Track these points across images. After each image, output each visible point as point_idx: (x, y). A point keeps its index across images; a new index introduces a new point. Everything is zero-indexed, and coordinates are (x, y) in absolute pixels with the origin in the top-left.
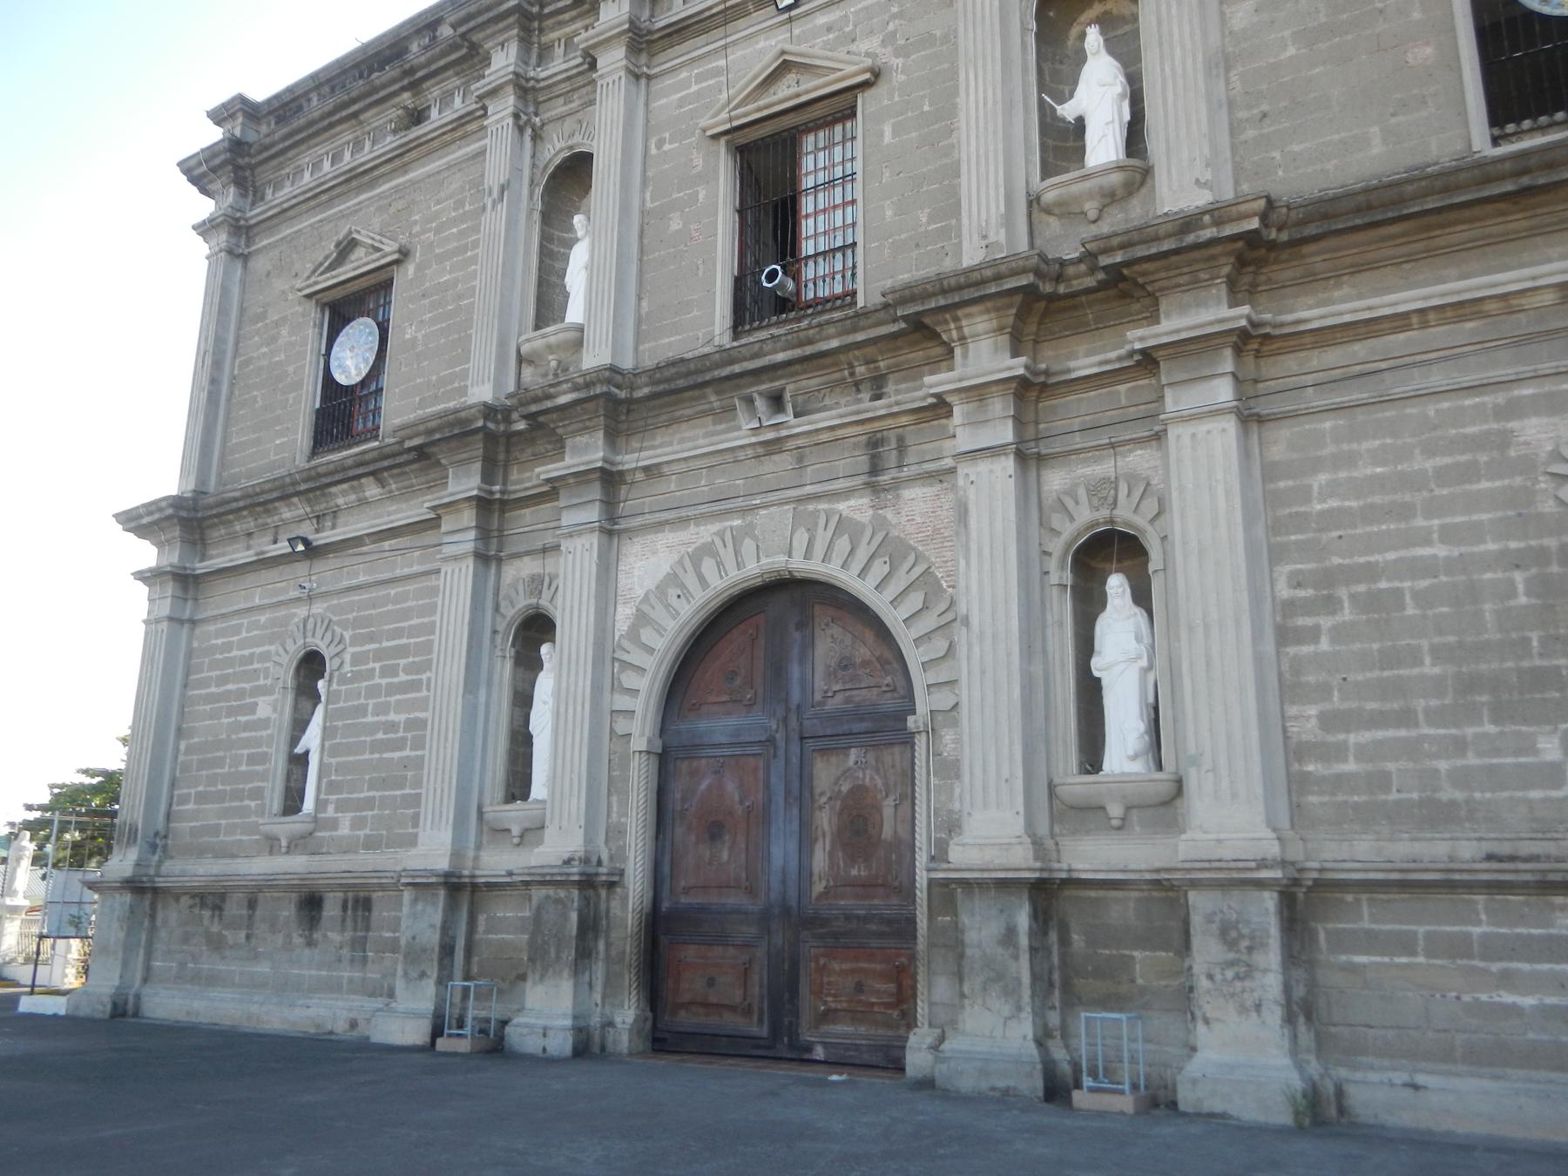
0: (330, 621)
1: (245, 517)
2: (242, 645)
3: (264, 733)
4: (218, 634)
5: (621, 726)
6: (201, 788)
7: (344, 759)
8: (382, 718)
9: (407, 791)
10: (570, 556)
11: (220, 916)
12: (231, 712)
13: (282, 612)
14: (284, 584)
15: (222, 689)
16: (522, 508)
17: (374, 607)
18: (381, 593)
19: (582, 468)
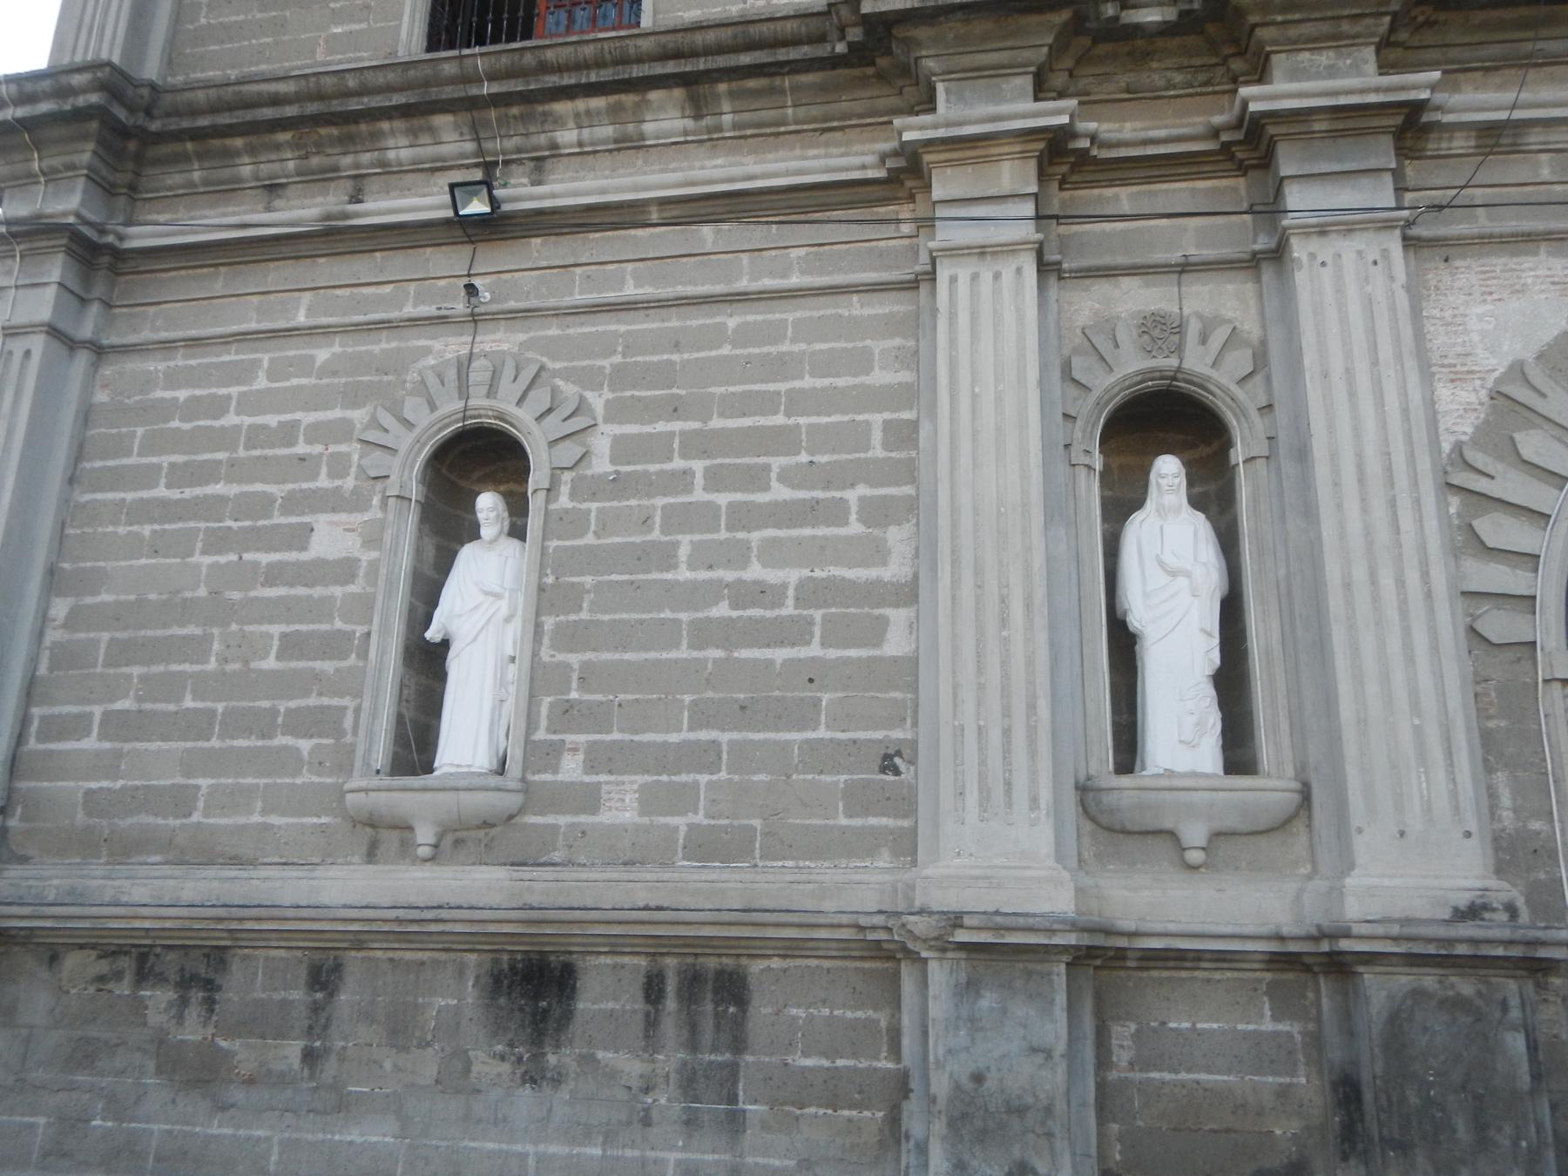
0: (542, 368)
1: (278, 147)
2: (249, 404)
3: (338, 591)
4: (173, 380)
5: (1500, 625)
7: (606, 656)
8: (729, 576)
9: (822, 733)
10: (1326, 274)
11: (210, 1004)
12: (218, 541)
13: (384, 344)
14: (388, 289)
15: (189, 493)
16: (1111, 183)
17: (677, 347)
18: (695, 323)
19: (1372, 98)
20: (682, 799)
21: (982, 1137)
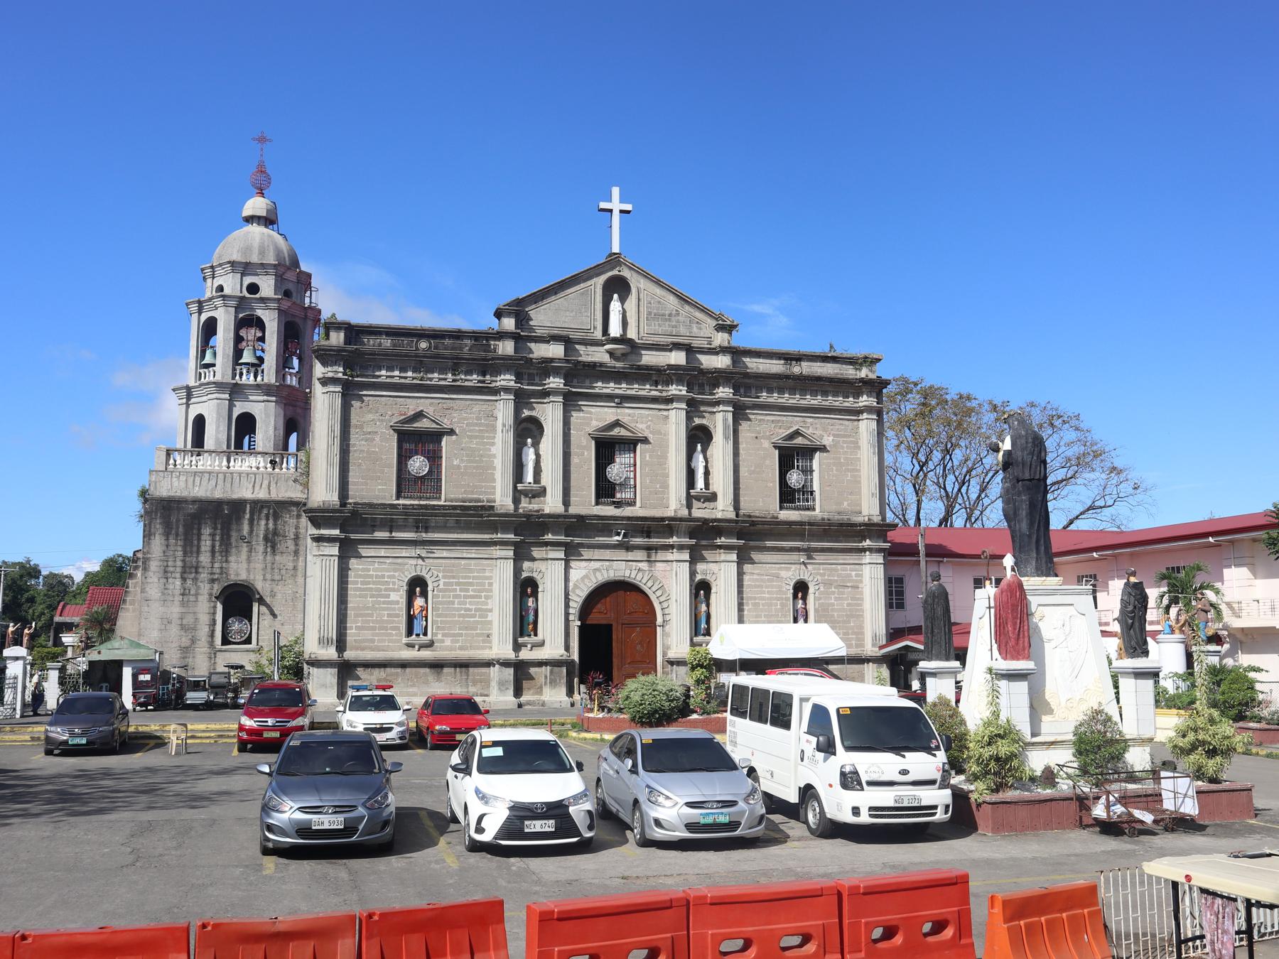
6: (359, 624)
20: (457, 641)
21: (502, 685)
